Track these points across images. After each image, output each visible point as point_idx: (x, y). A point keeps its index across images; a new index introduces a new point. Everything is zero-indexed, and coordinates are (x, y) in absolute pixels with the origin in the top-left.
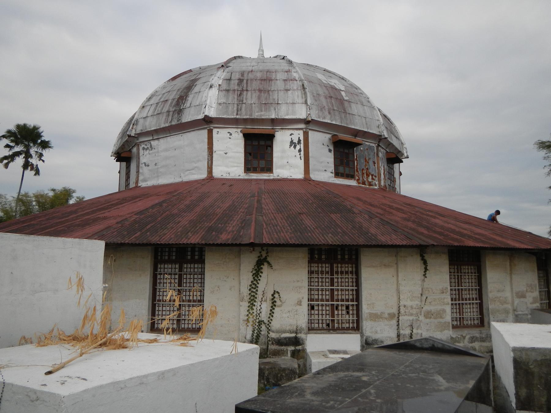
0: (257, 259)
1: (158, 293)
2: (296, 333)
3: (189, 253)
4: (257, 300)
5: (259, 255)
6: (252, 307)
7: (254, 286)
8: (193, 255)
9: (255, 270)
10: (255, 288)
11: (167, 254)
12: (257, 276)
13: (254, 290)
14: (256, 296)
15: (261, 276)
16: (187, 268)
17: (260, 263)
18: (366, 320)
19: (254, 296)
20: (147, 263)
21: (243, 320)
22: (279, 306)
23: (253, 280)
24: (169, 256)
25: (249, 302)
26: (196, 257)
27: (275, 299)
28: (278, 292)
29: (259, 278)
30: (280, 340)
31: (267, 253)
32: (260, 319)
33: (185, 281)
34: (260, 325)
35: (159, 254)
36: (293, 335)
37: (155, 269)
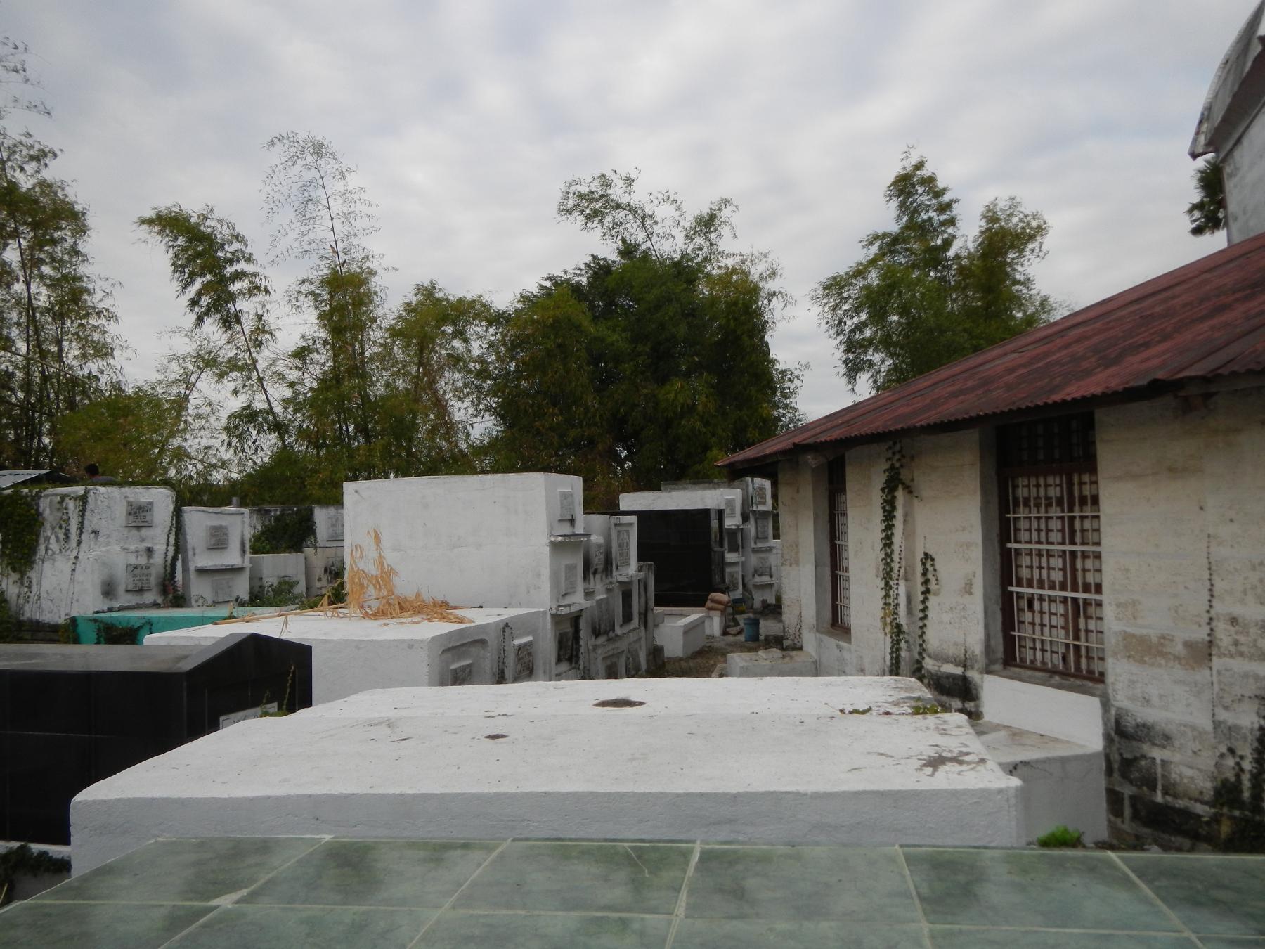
2: (965, 666)
5: (887, 466)
18: (1115, 654)
28: (933, 560)
36: (958, 671)
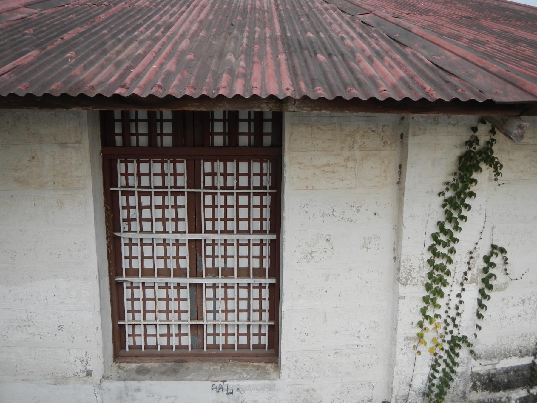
0: (458, 152)
1: (125, 251)
3: (218, 127)
4: (449, 279)
5: (467, 138)
6: (434, 301)
7: (443, 238)
8: (232, 134)
9: (455, 187)
10: (445, 245)
11: (143, 128)
12: (456, 208)
13: (445, 251)
14: (449, 267)
15: (468, 207)
16: (213, 174)
17: (469, 163)
19: (441, 268)
20: (76, 160)
21: (407, 338)
22: (500, 289)
23: (442, 218)
24: (152, 135)
25: (428, 287)
26: (243, 141)
27: (491, 271)
28: (503, 250)
29: (464, 212)
30: (494, 375)
31: (493, 132)
32: (455, 333)
33: (208, 213)
34: (452, 349)
35: (118, 129)
37: (109, 178)
